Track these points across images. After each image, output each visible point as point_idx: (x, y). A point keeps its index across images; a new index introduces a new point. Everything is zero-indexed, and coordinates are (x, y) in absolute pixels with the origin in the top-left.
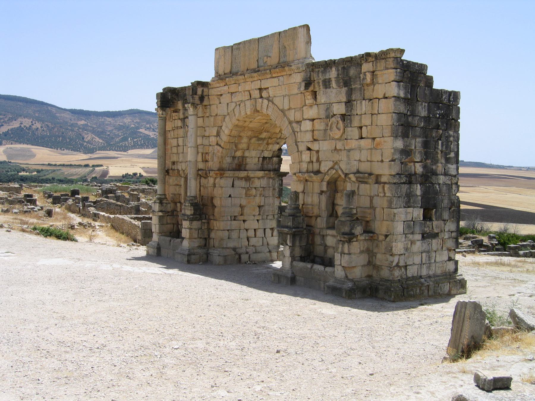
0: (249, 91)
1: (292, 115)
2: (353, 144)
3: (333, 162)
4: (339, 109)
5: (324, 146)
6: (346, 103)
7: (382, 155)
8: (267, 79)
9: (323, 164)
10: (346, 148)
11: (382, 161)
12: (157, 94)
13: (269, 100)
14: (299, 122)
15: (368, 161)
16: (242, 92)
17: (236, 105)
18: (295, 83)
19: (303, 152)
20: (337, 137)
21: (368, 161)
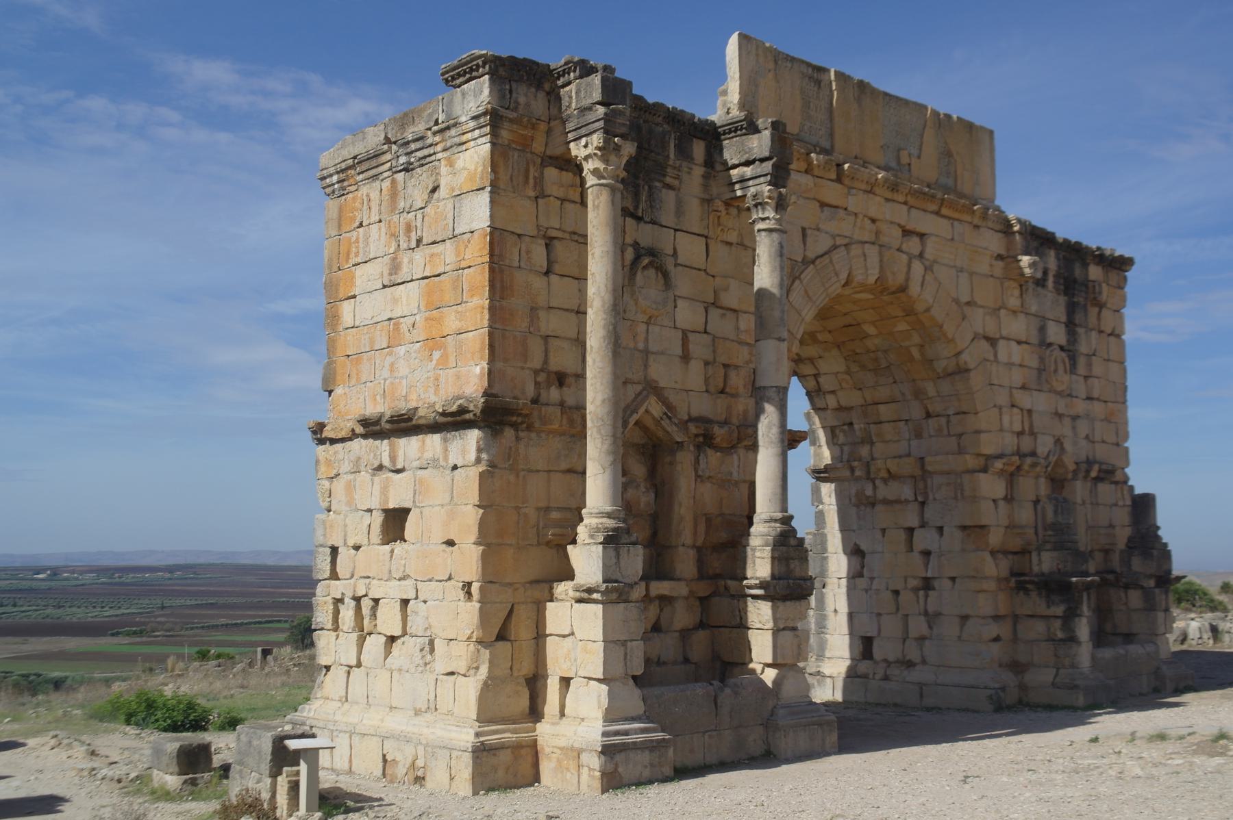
0: (873, 221)
1: (979, 321)
2: (1080, 407)
3: (1054, 436)
4: (1056, 333)
5: (1041, 403)
6: (1065, 323)
7: (1117, 434)
8: (925, 211)
9: (1040, 439)
10: (1071, 413)
11: (1117, 445)
12: (630, 83)
13: (926, 269)
14: (992, 341)
15: (1103, 442)
16: (861, 217)
17: (835, 247)
18: (986, 249)
19: (1004, 410)
20: (1059, 389)
21: (1103, 442)
